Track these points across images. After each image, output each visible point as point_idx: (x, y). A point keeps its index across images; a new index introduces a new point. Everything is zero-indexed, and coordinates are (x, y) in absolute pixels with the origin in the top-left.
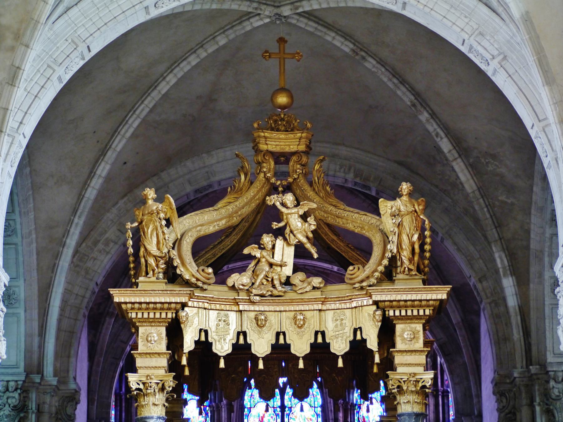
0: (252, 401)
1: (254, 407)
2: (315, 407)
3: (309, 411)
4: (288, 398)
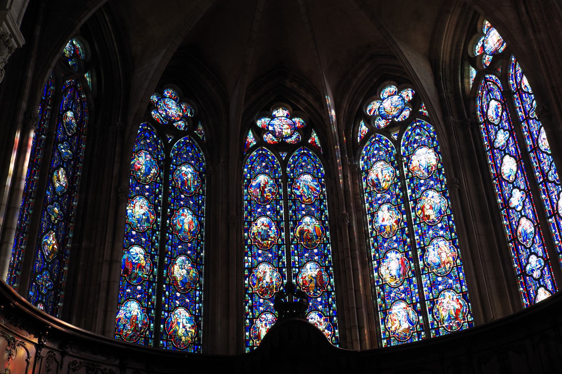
3: (313, 181)
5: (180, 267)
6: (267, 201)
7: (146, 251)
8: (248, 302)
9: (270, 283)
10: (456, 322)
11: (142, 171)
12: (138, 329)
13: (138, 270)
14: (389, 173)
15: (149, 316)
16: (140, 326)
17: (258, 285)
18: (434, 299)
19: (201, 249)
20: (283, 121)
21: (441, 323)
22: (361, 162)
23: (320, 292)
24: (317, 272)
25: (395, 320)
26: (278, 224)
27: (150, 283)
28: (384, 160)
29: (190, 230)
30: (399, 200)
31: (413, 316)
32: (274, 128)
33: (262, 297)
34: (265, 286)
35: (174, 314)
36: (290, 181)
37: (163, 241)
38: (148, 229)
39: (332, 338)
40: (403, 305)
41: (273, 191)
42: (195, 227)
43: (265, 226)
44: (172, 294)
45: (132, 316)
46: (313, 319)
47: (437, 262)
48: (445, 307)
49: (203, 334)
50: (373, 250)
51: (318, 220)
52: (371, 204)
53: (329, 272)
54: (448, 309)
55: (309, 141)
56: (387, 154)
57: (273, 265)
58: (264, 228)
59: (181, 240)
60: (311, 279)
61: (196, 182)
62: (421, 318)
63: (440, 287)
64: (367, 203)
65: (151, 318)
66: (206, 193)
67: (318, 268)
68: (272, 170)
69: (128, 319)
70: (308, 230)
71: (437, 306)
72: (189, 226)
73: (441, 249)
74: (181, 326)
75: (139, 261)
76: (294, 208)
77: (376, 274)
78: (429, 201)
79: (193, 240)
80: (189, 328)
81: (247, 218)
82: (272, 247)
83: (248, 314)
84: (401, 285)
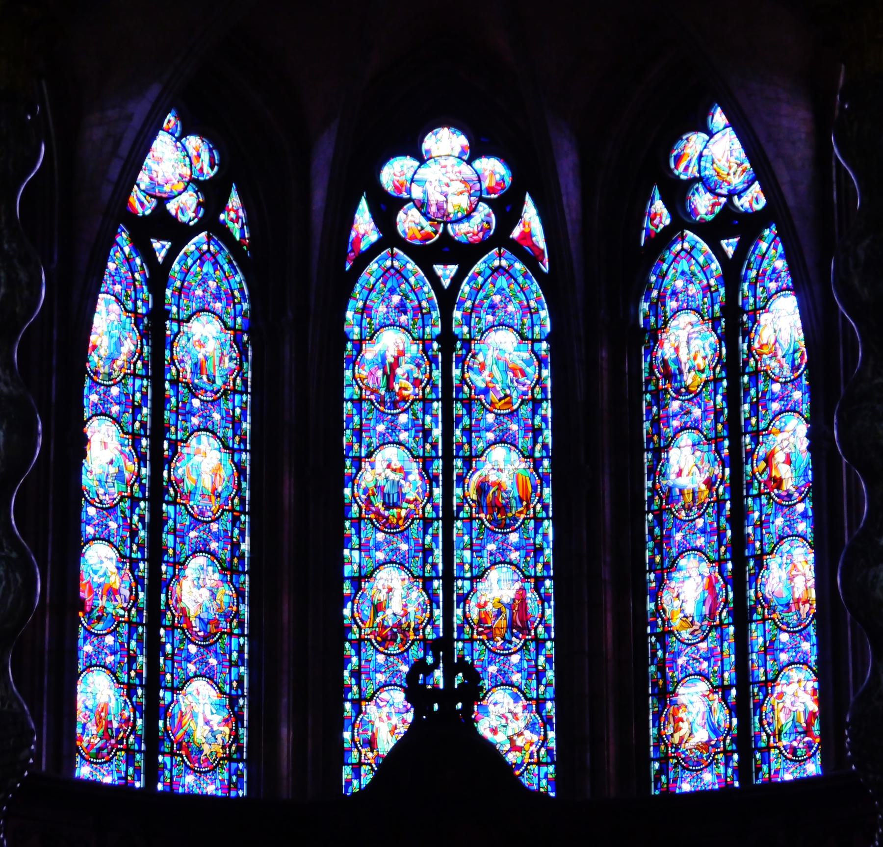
0: (365, 323)
1: (371, 338)
2: (534, 341)
4: (463, 317)
5: (196, 583)
6: (397, 402)
7: (119, 552)
8: (348, 660)
9: (403, 616)
10: (807, 739)
11: (102, 352)
12: (112, 732)
13: (105, 598)
14: (704, 349)
15: (132, 703)
16: (115, 725)
17: (374, 620)
18: (767, 681)
19: (242, 533)
20: (449, 169)
21: (774, 737)
22: (645, 306)
23: (518, 641)
24: (514, 591)
25: (683, 721)
26: (426, 462)
27: (133, 627)
28: (697, 311)
29: (214, 490)
30: (720, 427)
31: (721, 716)
32: (425, 192)
33: (381, 649)
34: (391, 624)
35: (185, 695)
36: (461, 349)
37: (157, 523)
38: (122, 498)
39: (538, 751)
40: (703, 687)
41: (416, 375)
42: (226, 479)
43: (394, 470)
44: (179, 649)
45: (98, 706)
46: (499, 706)
47: (784, 596)
48: (788, 704)
49: (249, 736)
50: (651, 544)
51: (524, 456)
52: (655, 424)
53: (542, 591)
54: (794, 709)
55: (516, 233)
56: (704, 296)
57: (411, 572)
58: (392, 476)
59: (195, 516)
60: (499, 609)
61: (226, 359)
62: (735, 721)
63: (784, 657)
64: (647, 420)
65: (136, 707)
66: (252, 387)
67: (518, 581)
68: (415, 315)
69: (91, 711)
70: (499, 484)
71: (772, 699)
72: (212, 477)
73: (795, 566)
74: (201, 721)
75: (107, 579)
76: (468, 422)
77: (651, 606)
78: (785, 443)
79: (222, 514)
80: (219, 724)
81: (350, 447)
82: (409, 526)
83: (350, 689)
84: (702, 641)
